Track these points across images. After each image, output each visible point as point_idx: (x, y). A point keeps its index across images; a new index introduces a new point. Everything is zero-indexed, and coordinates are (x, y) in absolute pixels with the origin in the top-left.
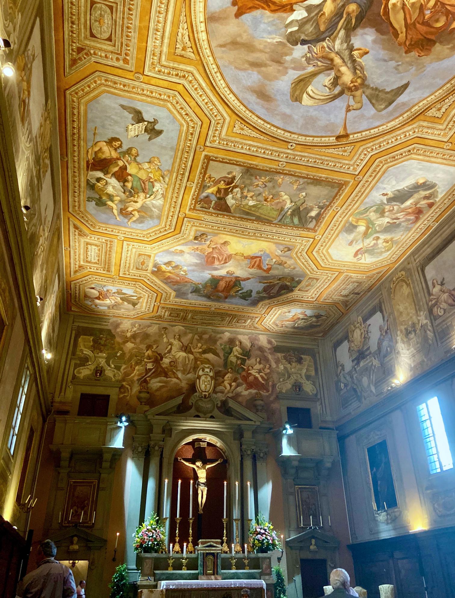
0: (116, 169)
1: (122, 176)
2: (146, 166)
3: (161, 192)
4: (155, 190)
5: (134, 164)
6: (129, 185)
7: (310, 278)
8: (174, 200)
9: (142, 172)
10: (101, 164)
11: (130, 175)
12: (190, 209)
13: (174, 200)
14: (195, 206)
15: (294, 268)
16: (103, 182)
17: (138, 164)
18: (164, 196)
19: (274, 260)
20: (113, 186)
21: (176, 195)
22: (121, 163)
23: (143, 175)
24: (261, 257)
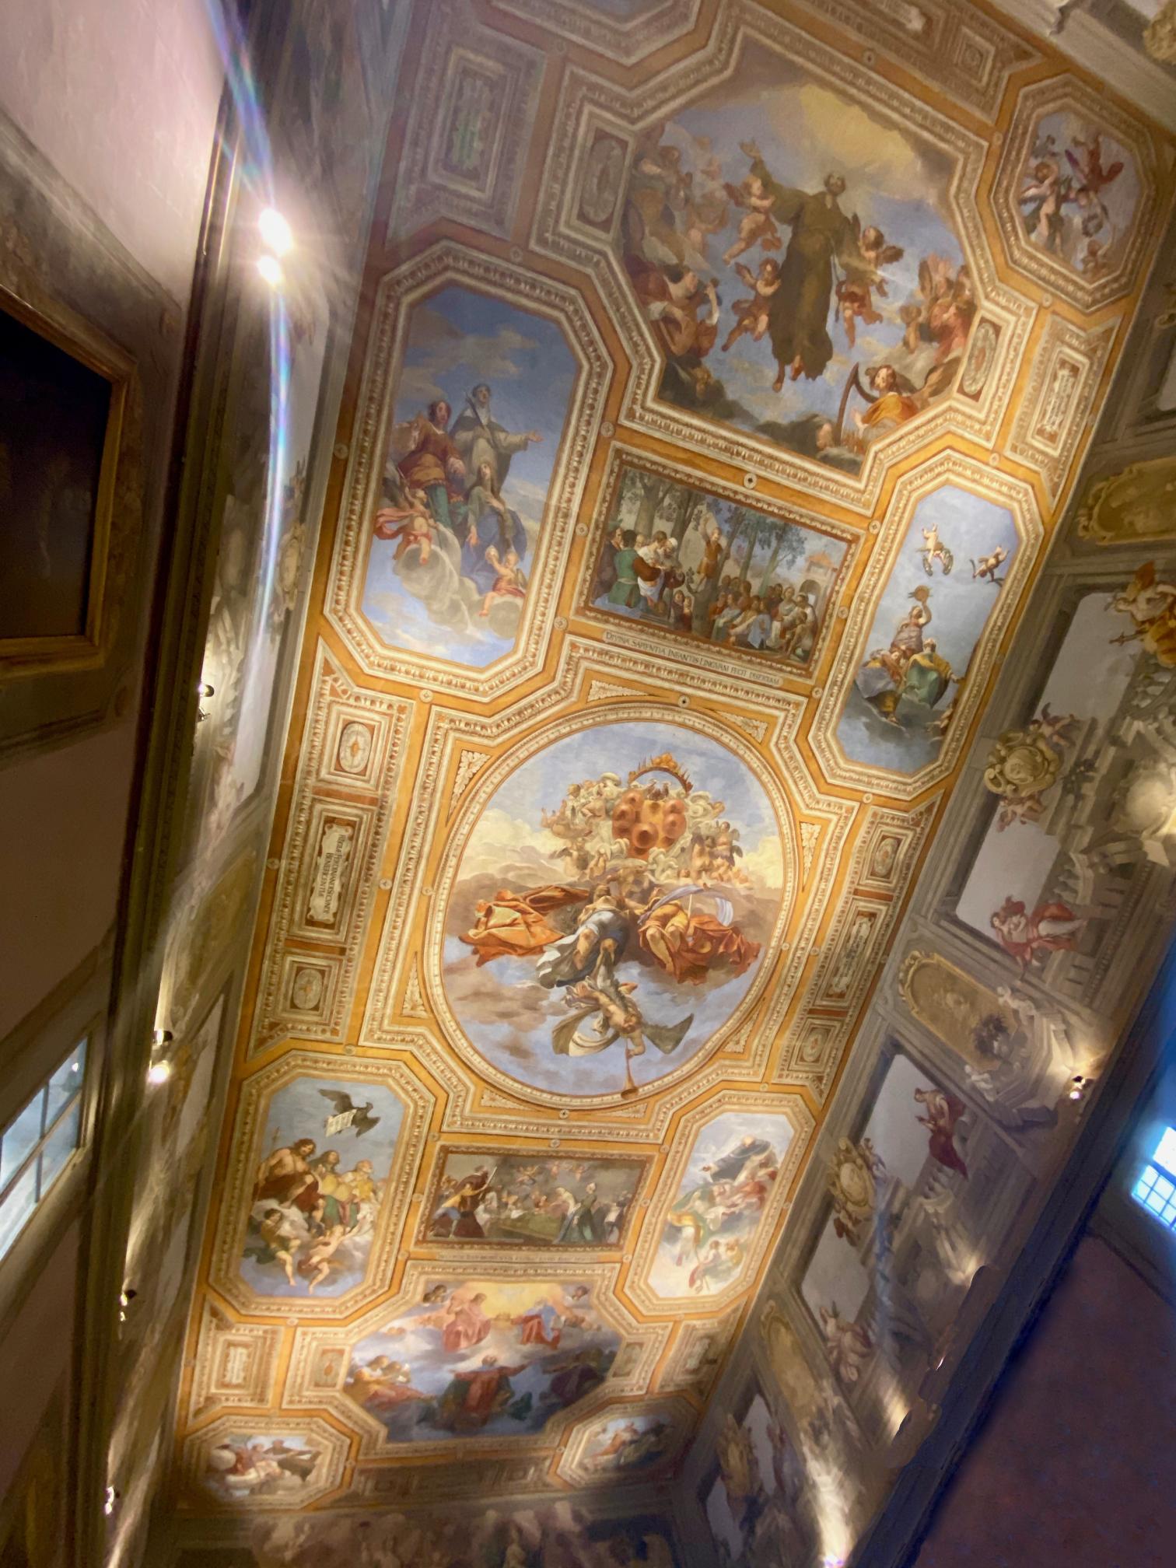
0: (301, 1190)
1: (307, 1203)
2: (350, 1176)
3: (370, 1218)
4: (360, 1216)
5: (330, 1178)
6: (318, 1215)
7: (629, 1345)
8: (391, 1229)
9: (342, 1188)
10: (278, 1186)
11: (323, 1197)
12: (418, 1242)
13: (391, 1229)
14: (424, 1236)
15: (599, 1328)
16: (276, 1217)
17: (337, 1175)
18: (374, 1225)
19: (563, 1318)
20: (291, 1220)
21: (394, 1219)
22: (309, 1179)
23: (342, 1195)
24: (537, 1316)
